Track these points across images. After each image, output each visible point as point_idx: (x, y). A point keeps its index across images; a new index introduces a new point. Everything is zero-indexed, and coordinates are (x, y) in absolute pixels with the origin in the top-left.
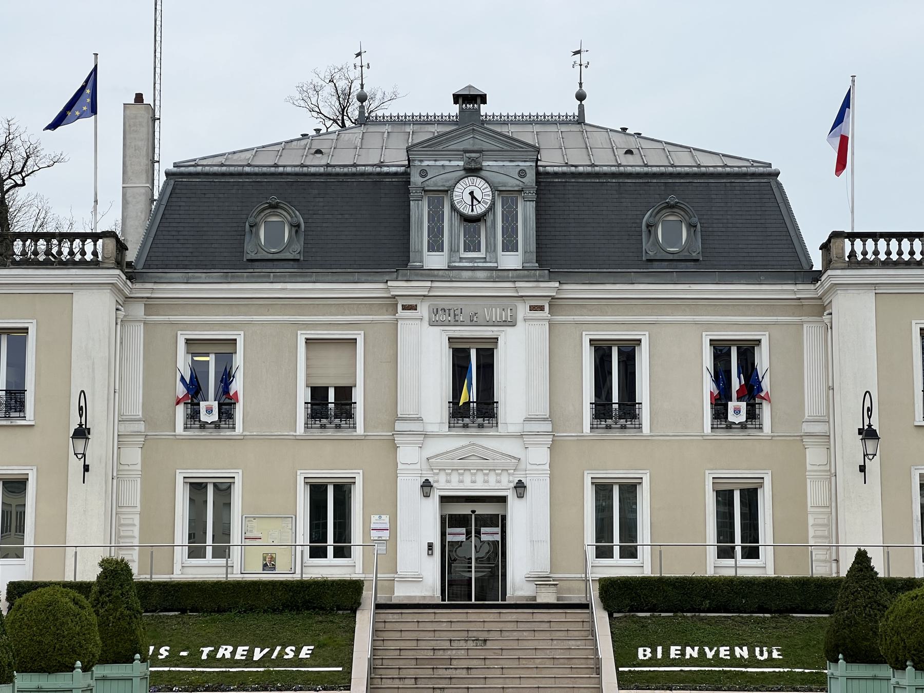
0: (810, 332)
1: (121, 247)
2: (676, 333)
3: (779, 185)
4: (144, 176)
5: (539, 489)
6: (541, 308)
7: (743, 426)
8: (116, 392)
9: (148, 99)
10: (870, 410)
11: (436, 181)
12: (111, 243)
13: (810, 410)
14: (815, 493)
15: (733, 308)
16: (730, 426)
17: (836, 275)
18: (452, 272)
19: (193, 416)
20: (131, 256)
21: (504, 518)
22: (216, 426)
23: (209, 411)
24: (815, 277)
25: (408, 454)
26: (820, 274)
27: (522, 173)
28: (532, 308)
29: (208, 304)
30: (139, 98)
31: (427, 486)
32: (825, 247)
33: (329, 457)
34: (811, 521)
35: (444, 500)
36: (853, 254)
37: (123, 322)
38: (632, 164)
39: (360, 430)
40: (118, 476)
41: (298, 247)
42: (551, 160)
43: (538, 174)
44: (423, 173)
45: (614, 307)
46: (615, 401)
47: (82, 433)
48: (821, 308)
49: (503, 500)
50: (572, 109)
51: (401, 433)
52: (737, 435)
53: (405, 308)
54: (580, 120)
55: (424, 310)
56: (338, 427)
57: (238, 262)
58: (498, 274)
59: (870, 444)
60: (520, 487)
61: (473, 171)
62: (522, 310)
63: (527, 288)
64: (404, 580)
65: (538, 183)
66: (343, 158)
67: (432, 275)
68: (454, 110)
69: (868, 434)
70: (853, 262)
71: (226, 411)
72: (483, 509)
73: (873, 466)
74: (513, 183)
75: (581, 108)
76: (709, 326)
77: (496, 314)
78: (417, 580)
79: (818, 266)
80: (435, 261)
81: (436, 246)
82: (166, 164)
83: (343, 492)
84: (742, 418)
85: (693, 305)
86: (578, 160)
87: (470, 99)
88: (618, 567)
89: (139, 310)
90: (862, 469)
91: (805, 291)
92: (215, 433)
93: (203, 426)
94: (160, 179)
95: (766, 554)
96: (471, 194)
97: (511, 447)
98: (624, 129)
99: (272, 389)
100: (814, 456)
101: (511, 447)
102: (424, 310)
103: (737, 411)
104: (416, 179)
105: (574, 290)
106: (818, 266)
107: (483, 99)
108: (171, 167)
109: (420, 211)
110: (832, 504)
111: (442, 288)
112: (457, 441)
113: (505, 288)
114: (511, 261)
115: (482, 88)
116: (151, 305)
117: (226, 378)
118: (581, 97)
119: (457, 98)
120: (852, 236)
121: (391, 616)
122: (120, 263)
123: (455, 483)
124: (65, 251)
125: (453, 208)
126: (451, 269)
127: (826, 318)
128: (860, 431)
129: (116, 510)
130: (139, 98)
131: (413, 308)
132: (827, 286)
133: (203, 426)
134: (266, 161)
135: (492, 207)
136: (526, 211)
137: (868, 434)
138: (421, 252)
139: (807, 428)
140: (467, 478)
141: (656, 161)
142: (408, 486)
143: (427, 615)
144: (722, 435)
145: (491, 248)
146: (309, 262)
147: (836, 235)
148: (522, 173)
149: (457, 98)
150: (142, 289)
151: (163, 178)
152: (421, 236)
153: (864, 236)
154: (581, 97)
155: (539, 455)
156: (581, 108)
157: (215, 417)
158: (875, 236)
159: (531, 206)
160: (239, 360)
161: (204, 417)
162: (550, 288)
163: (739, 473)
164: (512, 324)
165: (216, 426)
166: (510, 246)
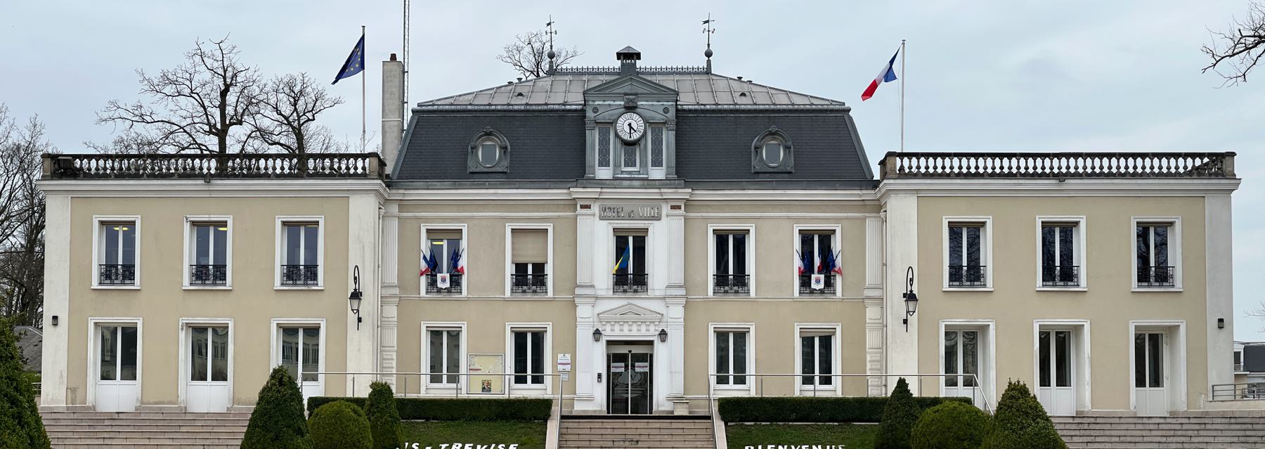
0: (871, 225)
1: (382, 164)
2: (774, 227)
3: (850, 119)
4: (397, 114)
6: (679, 207)
7: (822, 292)
8: (380, 266)
9: (399, 58)
10: (912, 280)
11: (604, 116)
12: (375, 161)
13: (870, 280)
14: (872, 339)
15: (817, 206)
16: (812, 292)
17: (889, 183)
18: (615, 181)
19: (433, 283)
20: (389, 170)
21: (651, 356)
22: (449, 291)
23: (444, 280)
24: (875, 185)
25: (585, 312)
26: (878, 182)
27: (666, 110)
28: (673, 207)
29: (443, 204)
30: (393, 57)
31: (597, 334)
32: (882, 163)
34: (868, 358)
35: (609, 343)
36: (902, 168)
37: (384, 217)
38: (745, 103)
39: (550, 294)
40: (381, 325)
41: (506, 163)
42: (687, 101)
43: (677, 110)
44: (595, 110)
45: (729, 206)
46: (731, 275)
48: (878, 207)
49: (651, 343)
50: (702, 63)
51: (580, 296)
52: (817, 298)
53: (582, 207)
54: (708, 71)
55: (596, 208)
56: (535, 292)
57: (463, 175)
58: (648, 183)
59: (911, 304)
60: (663, 335)
61: (631, 108)
62: (666, 209)
63: (669, 193)
64: (581, 399)
65: (677, 117)
66: (538, 99)
67: (601, 183)
68: (617, 64)
69: (910, 297)
70: (902, 174)
73: (913, 320)
74: (659, 117)
75: (709, 62)
76: (798, 220)
77: (647, 211)
78: (590, 399)
79: (877, 177)
80: (604, 173)
81: (604, 162)
82: (412, 104)
83: (538, 338)
84: (822, 286)
86: (706, 100)
87: (629, 56)
89: (394, 209)
90: (905, 322)
91: (868, 194)
92: (447, 296)
93: (439, 291)
94: (408, 115)
95: (837, 381)
96: (630, 126)
97: (657, 306)
98: (740, 78)
99: (488, 264)
100: (872, 313)
101: (657, 306)
102: (596, 208)
103: (818, 281)
104: (590, 114)
105: (703, 195)
106: (877, 177)
107: (638, 56)
108: (416, 107)
109: (593, 137)
110: (883, 347)
111: (609, 193)
112: (619, 302)
113: (652, 193)
114: (658, 173)
115: (637, 48)
116: (403, 205)
117: (455, 257)
118: (709, 54)
119: (619, 55)
120: (902, 155)
121: (571, 424)
122: (381, 175)
123: (617, 332)
124: (343, 167)
125: (617, 135)
126: (615, 179)
127: (882, 214)
128: (905, 295)
129: (380, 349)
130: (393, 57)
131: (588, 207)
132: (883, 191)
133: (439, 291)
134: (483, 101)
135: (644, 135)
136: (668, 137)
137: (910, 297)
138: (594, 167)
139: (867, 293)
140: (626, 328)
141: (762, 101)
143: (597, 424)
144: (807, 298)
145: (644, 164)
146: (513, 174)
147: (890, 155)
148: (666, 110)
149: (619, 55)
150: (397, 194)
151: (410, 114)
152: (593, 155)
153: (910, 155)
154: (709, 54)
156: (709, 62)
157: (447, 285)
158: (918, 155)
160: (464, 244)
161: (440, 285)
162: (685, 193)
163: (818, 325)
164: (659, 219)
165: (449, 291)
166: (657, 163)
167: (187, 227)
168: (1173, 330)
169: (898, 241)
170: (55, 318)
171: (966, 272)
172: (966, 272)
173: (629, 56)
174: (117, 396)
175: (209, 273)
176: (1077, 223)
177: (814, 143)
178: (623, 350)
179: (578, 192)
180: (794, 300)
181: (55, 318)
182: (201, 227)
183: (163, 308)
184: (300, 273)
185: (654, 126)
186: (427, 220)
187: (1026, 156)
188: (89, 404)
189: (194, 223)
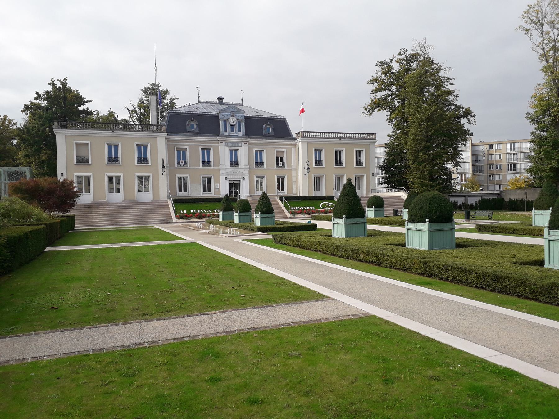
0: (293, 149)
5: (247, 178)
11: (226, 118)
14: (294, 179)
18: (229, 136)
21: (239, 184)
22: (183, 166)
24: (294, 139)
25: (222, 172)
31: (226, 178)
33: (205, 173)
38: (259, 115)
39: (213, 167)
45: (260, 143)
47: (163, 167)
48: (295, 145)
50: (240, 102)
54: (242, 105)
55: (224, 144)
57: (184, 131)
58: (238, 137)
60: (243, 178)
61: (233, 116)
62: (243, 144)
63: (244, 140)
68: (217, 101)
71: (185, 163)
72: (235, 182)
74: (240, 118)
76: (276, 148)
77: (239, 145)
80: (226, 133)
81: (225, 130)
85: (273, 144)
87: (221, 99)
88: (281, 193)
93: (181, 166)
96: (233, 121)
99: (194, 157)
100: (294, 172)
101: (242, 171)
102: (224, 144)
104: (220, 117)
105: (253, 141)
109: (221, 123)
111: (230, 139)
113: (240, 140)
114: (240, 134)
118: (242, 100)
133: (181, 166)
136: (243, 125)
142: (222, 179)
144: (278, 169)
146: (202, 132)
154: (242, 100)
155: (247, 172)
159: (244, 124)
162: (248, 140)
163: (280, 176)
165: (183, 166)
166: (239, 131)
167: (106, 146)
168: (362, 176)
169: (299, 154)
170: (62, 174)
171: (318, 163)
172: (318, 163)
173: (221, 99)
174: (118, 198)
175: (113, 159)
176: (322, 150)
177: (278, 128)
178: (232, 182)
179: (218, 139)
180: (276, 169)
181: (62, 174)
182: (110, 146)
183: (128, 169)
184: (142, 160)
185: (239, 122)
186: (176, 145)
187: (332, 133)
188: (107, 199)
189: (107, 144)
